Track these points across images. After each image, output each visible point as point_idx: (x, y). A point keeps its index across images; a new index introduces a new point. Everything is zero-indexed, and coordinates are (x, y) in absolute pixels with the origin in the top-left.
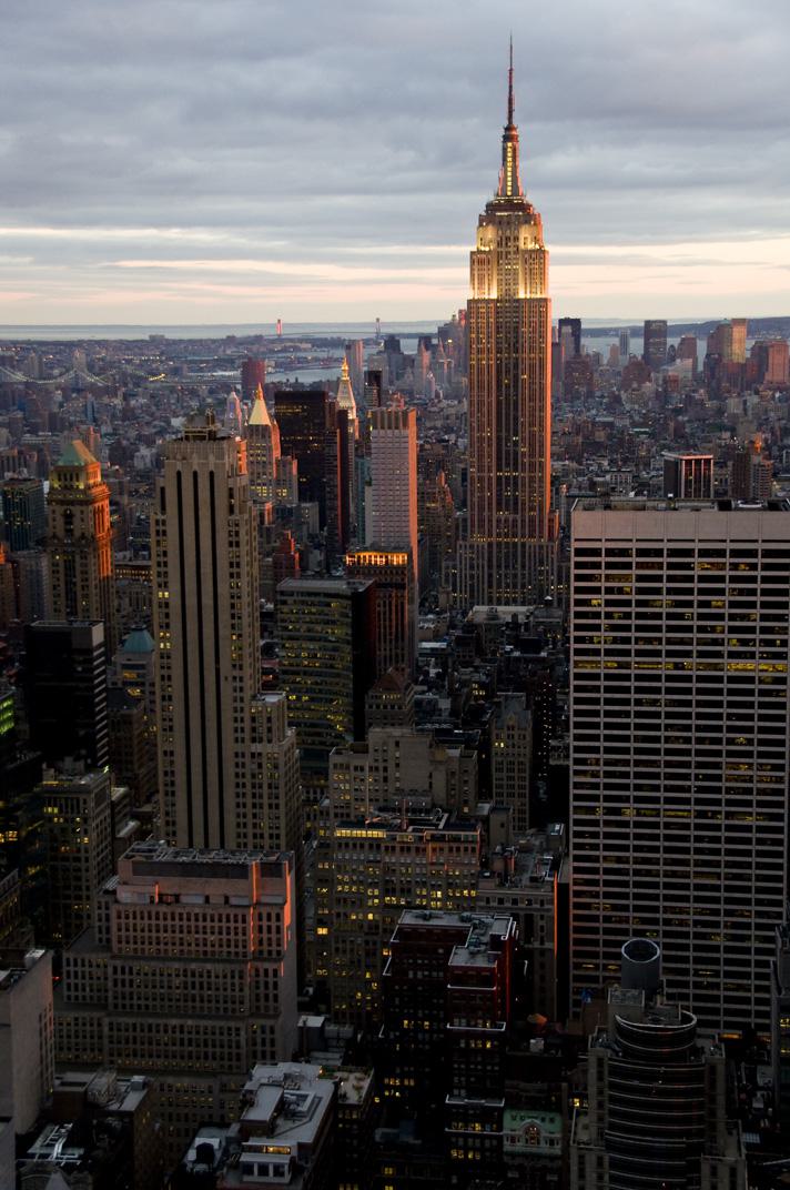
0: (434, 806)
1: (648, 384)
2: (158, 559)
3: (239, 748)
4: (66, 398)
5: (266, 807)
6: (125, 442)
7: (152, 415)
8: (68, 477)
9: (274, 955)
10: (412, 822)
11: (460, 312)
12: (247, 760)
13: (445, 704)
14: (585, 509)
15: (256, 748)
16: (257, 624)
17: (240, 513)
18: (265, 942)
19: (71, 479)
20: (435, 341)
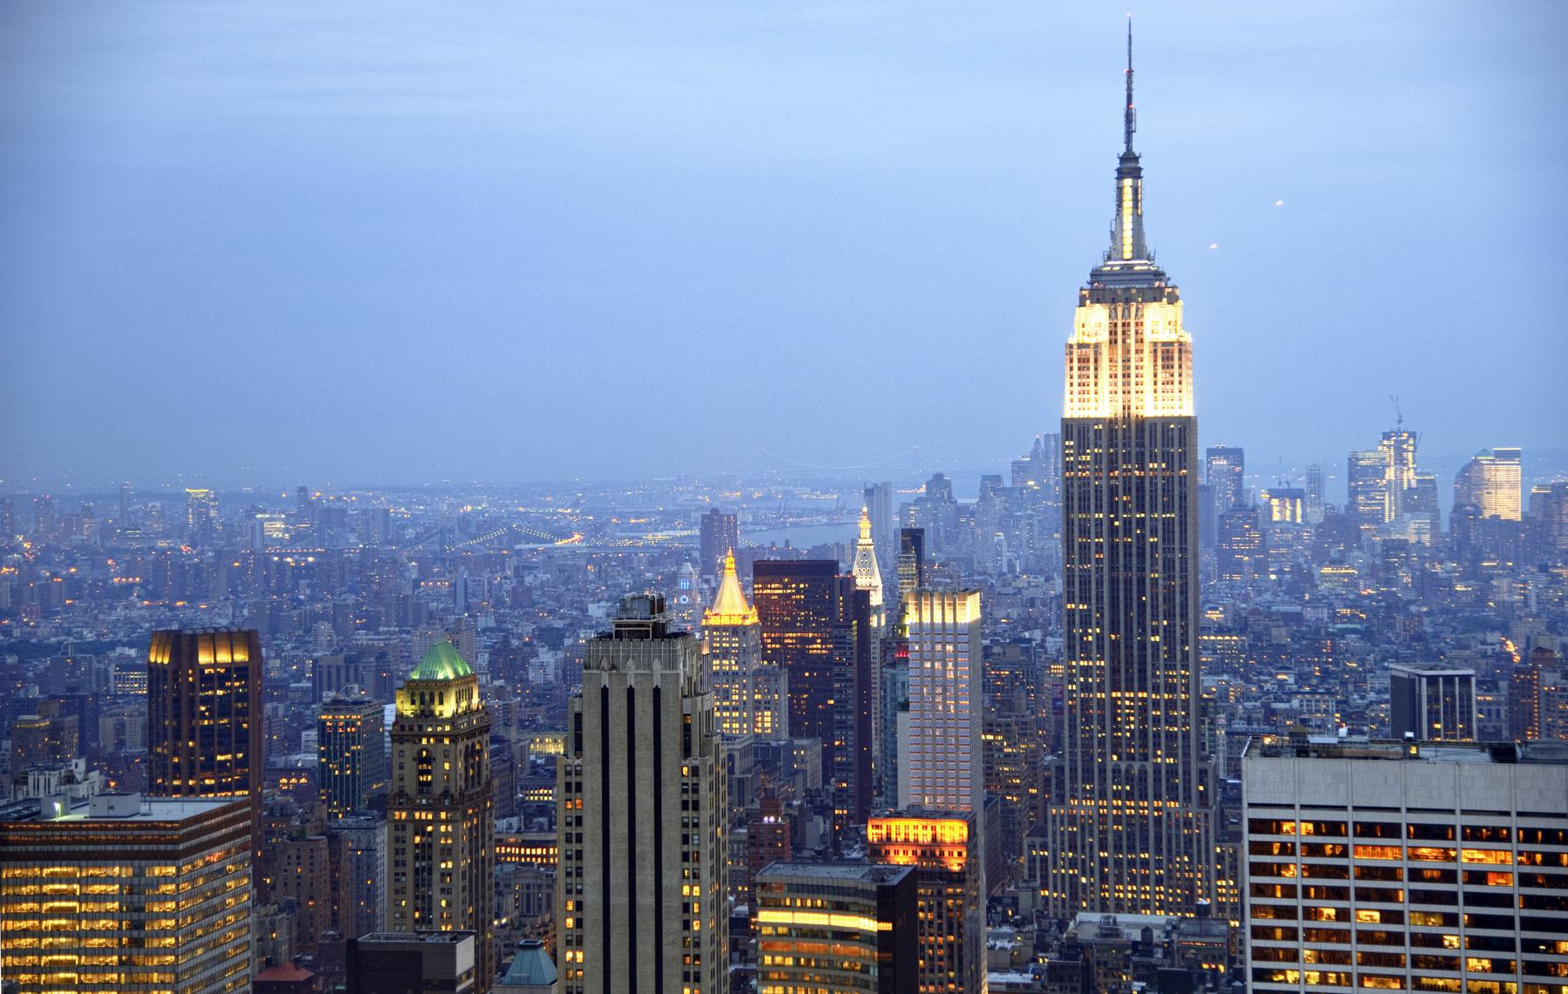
1: (1356, 553)
2: (568, 830)
4: (425, 573)
6: (515, 643)
7: (558, 599)
8: (427, 698)
11: (1047, 436)
14: (1264, 755)
16: (725, 940)
17: (702, 755)
19: (432, 701)
20: (1007, 483)
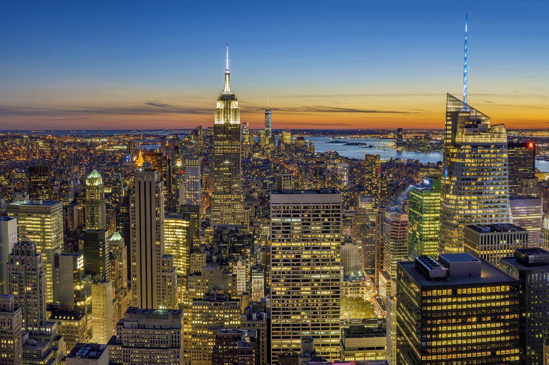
0: (225, 293)
3: (159, 274)
5: (167, 294)
9: (177, 346)
10: (218, 299)
12: (161, 278)
13: (215, 258)
15: (164, 274)
18: (174, 341)
